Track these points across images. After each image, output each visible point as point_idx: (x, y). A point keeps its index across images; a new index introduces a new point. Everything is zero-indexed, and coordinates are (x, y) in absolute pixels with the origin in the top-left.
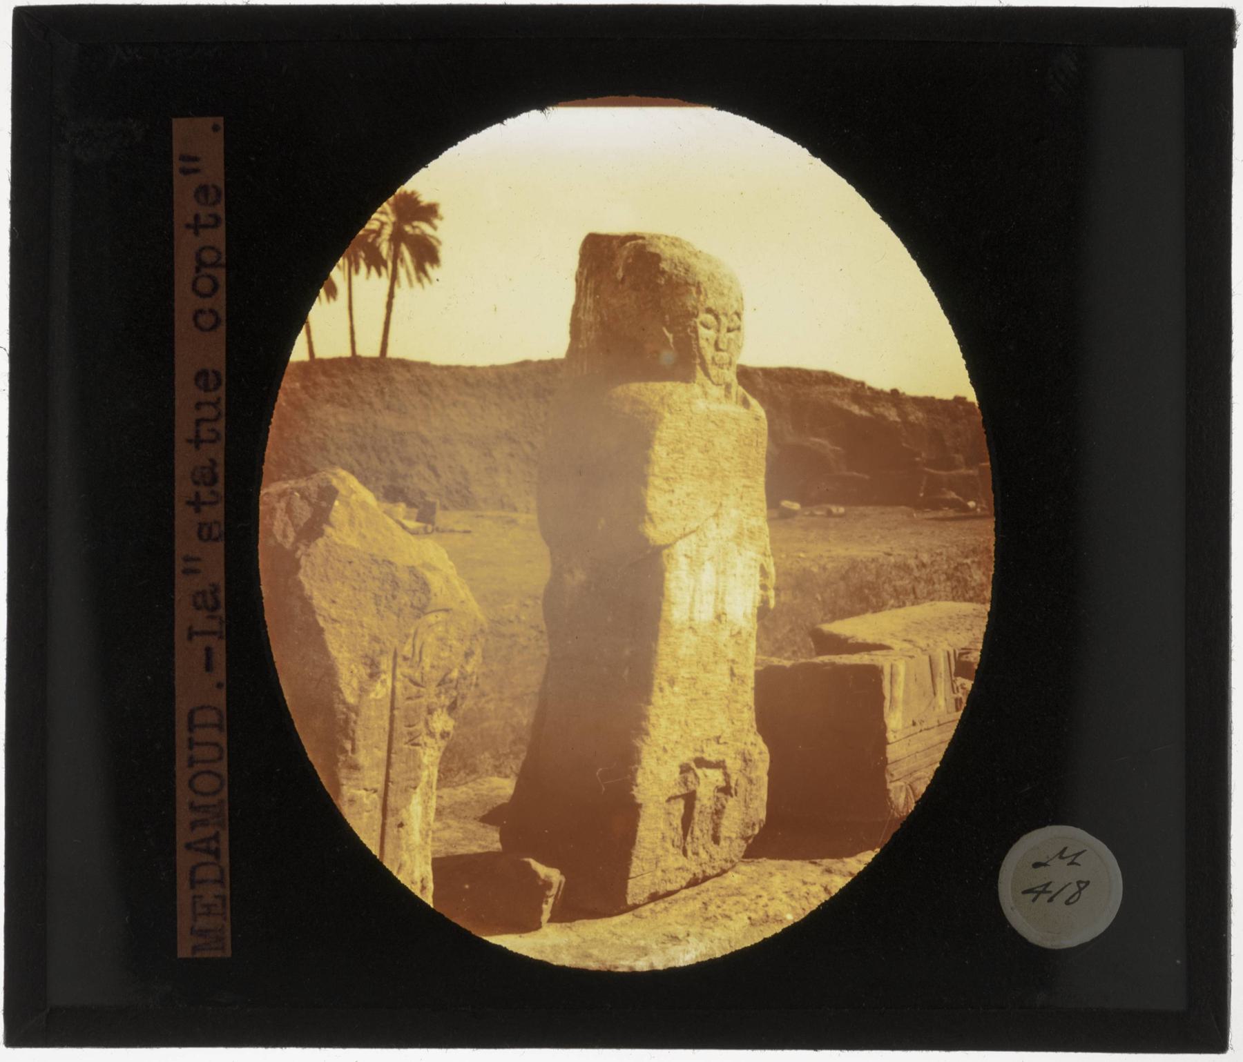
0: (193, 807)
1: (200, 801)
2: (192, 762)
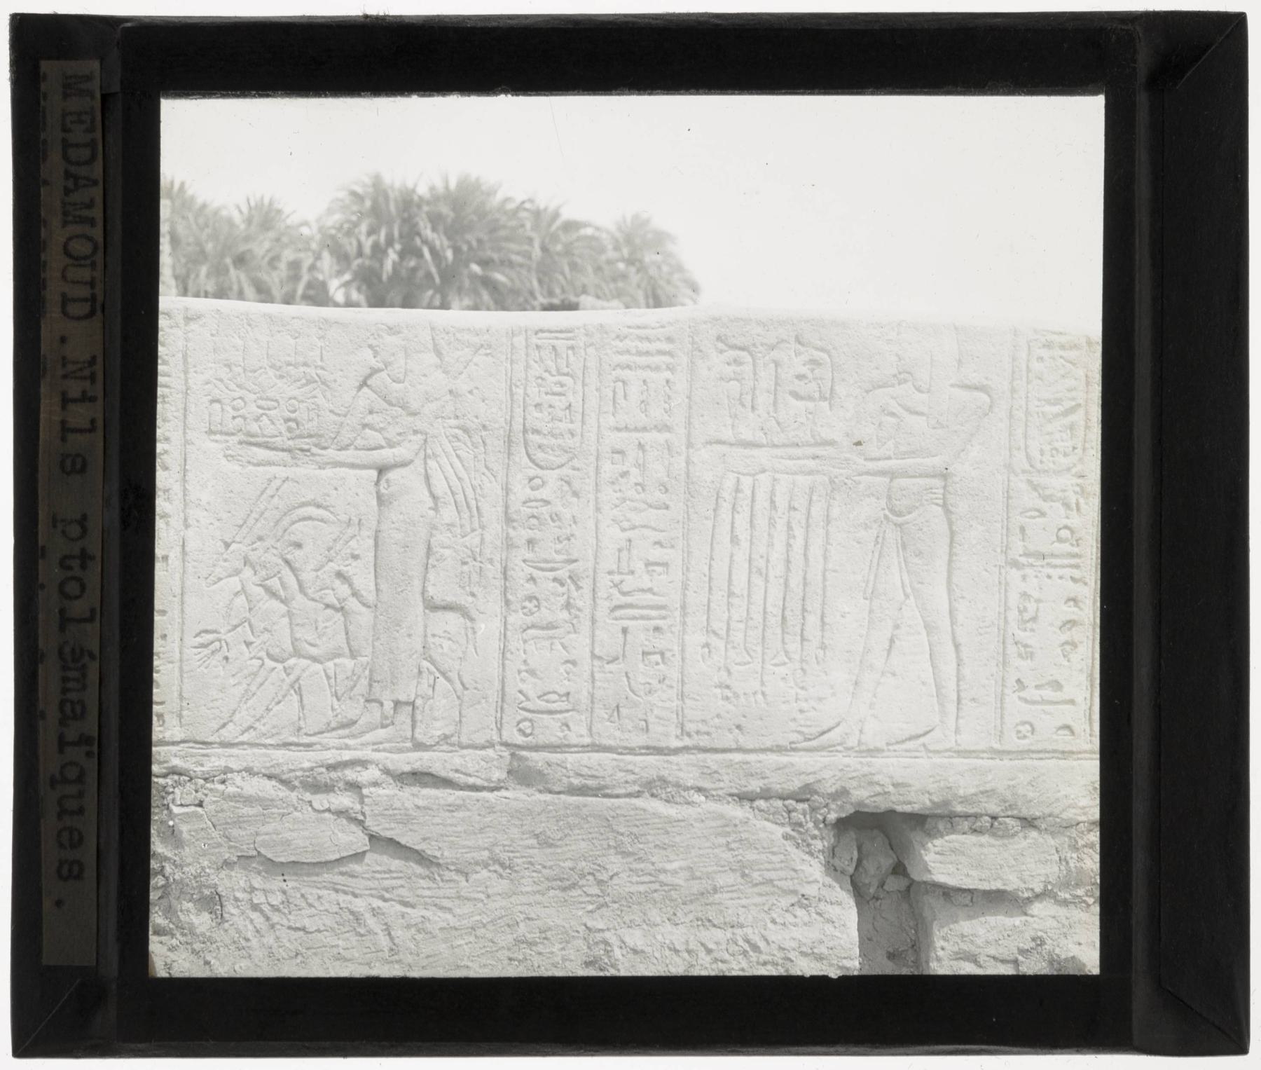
1: (86, 229)
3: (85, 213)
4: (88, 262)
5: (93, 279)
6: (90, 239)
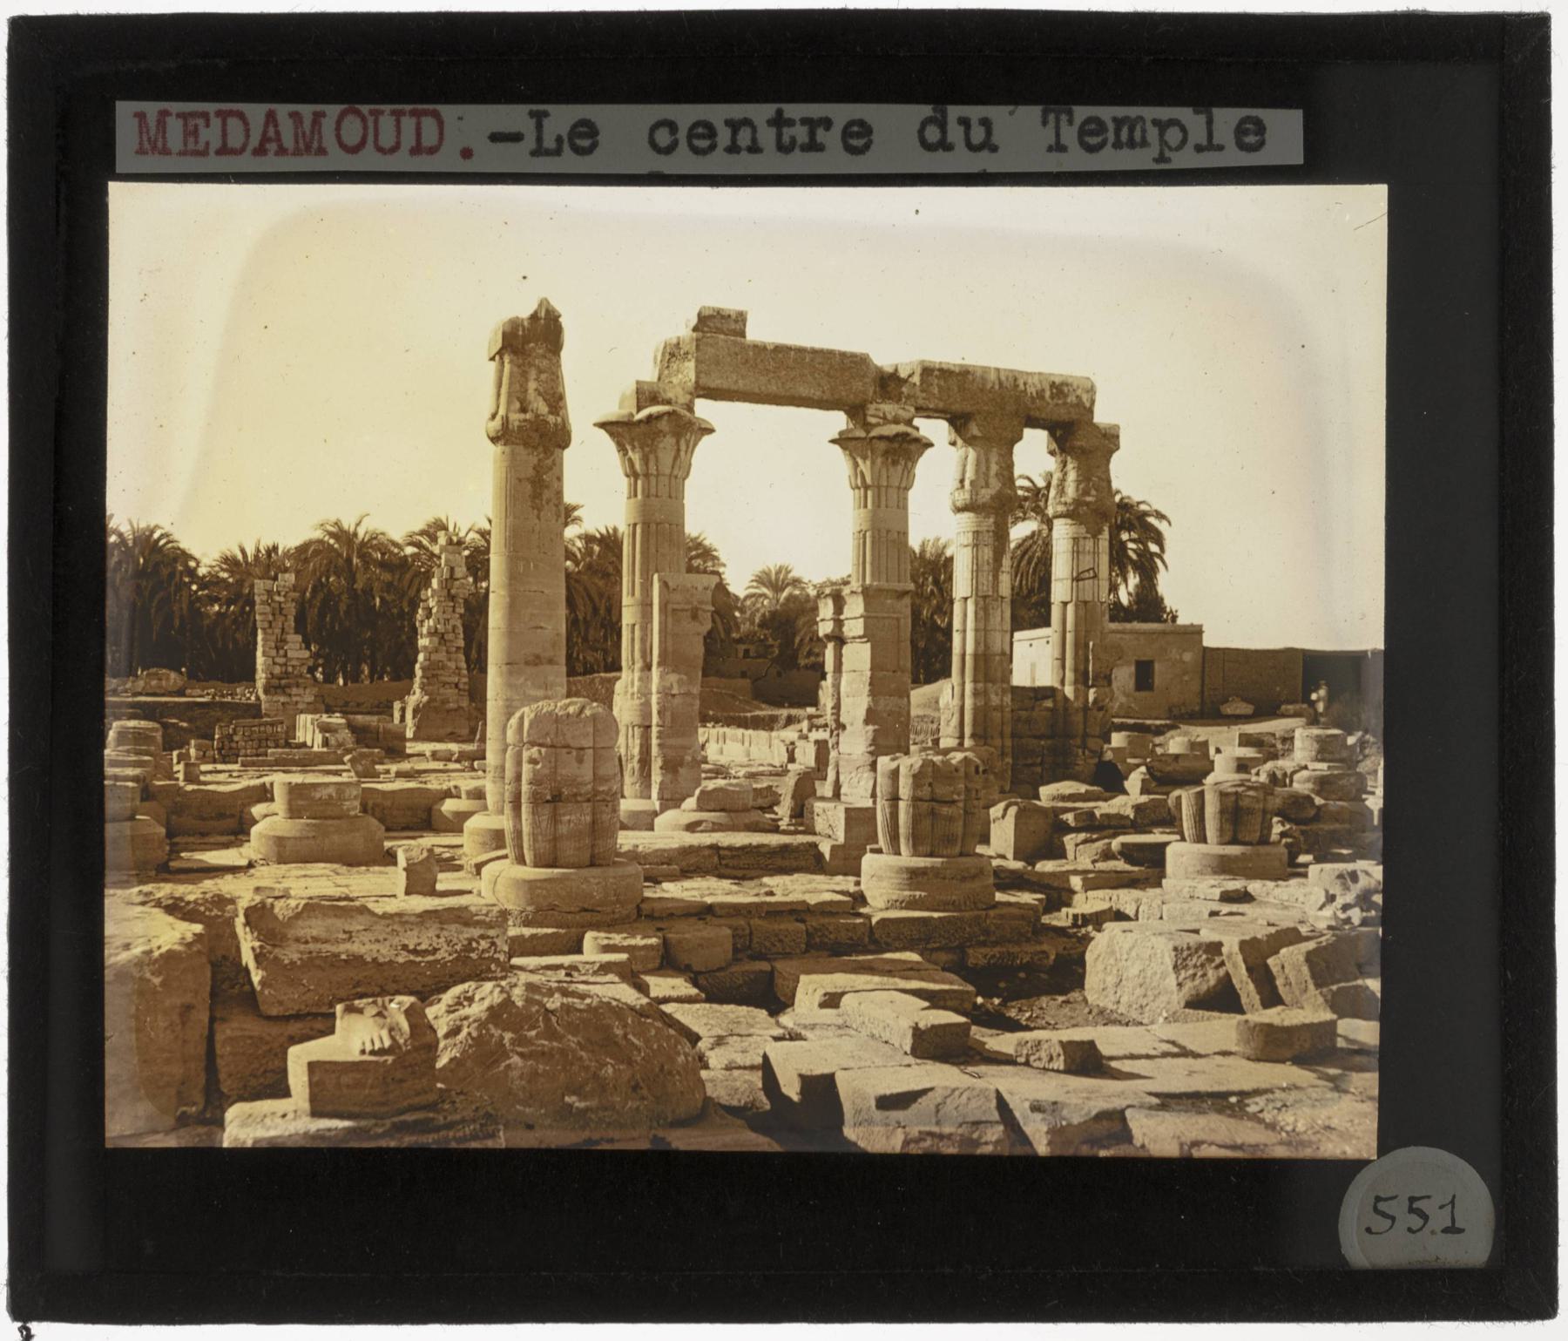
0: (318, 116)
4: (371, 120)
5: (393, 113)
6: (343, 115)
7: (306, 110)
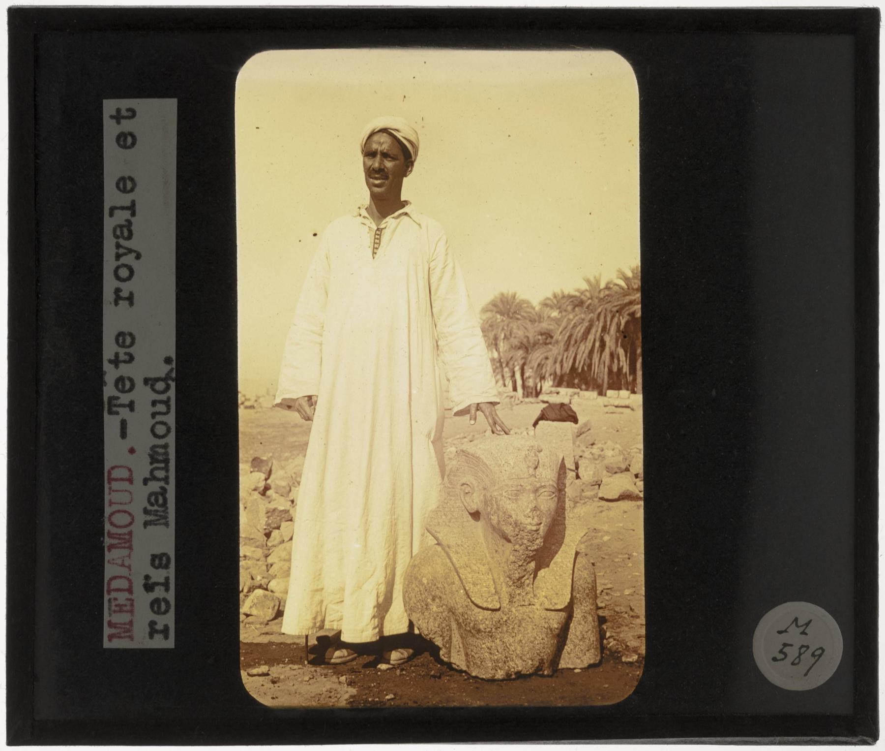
0: (110, 535)
2: (111, 503)
3: (115, 541)
4: (115, 507)
6: (112, 524)
7: (107, 541)
